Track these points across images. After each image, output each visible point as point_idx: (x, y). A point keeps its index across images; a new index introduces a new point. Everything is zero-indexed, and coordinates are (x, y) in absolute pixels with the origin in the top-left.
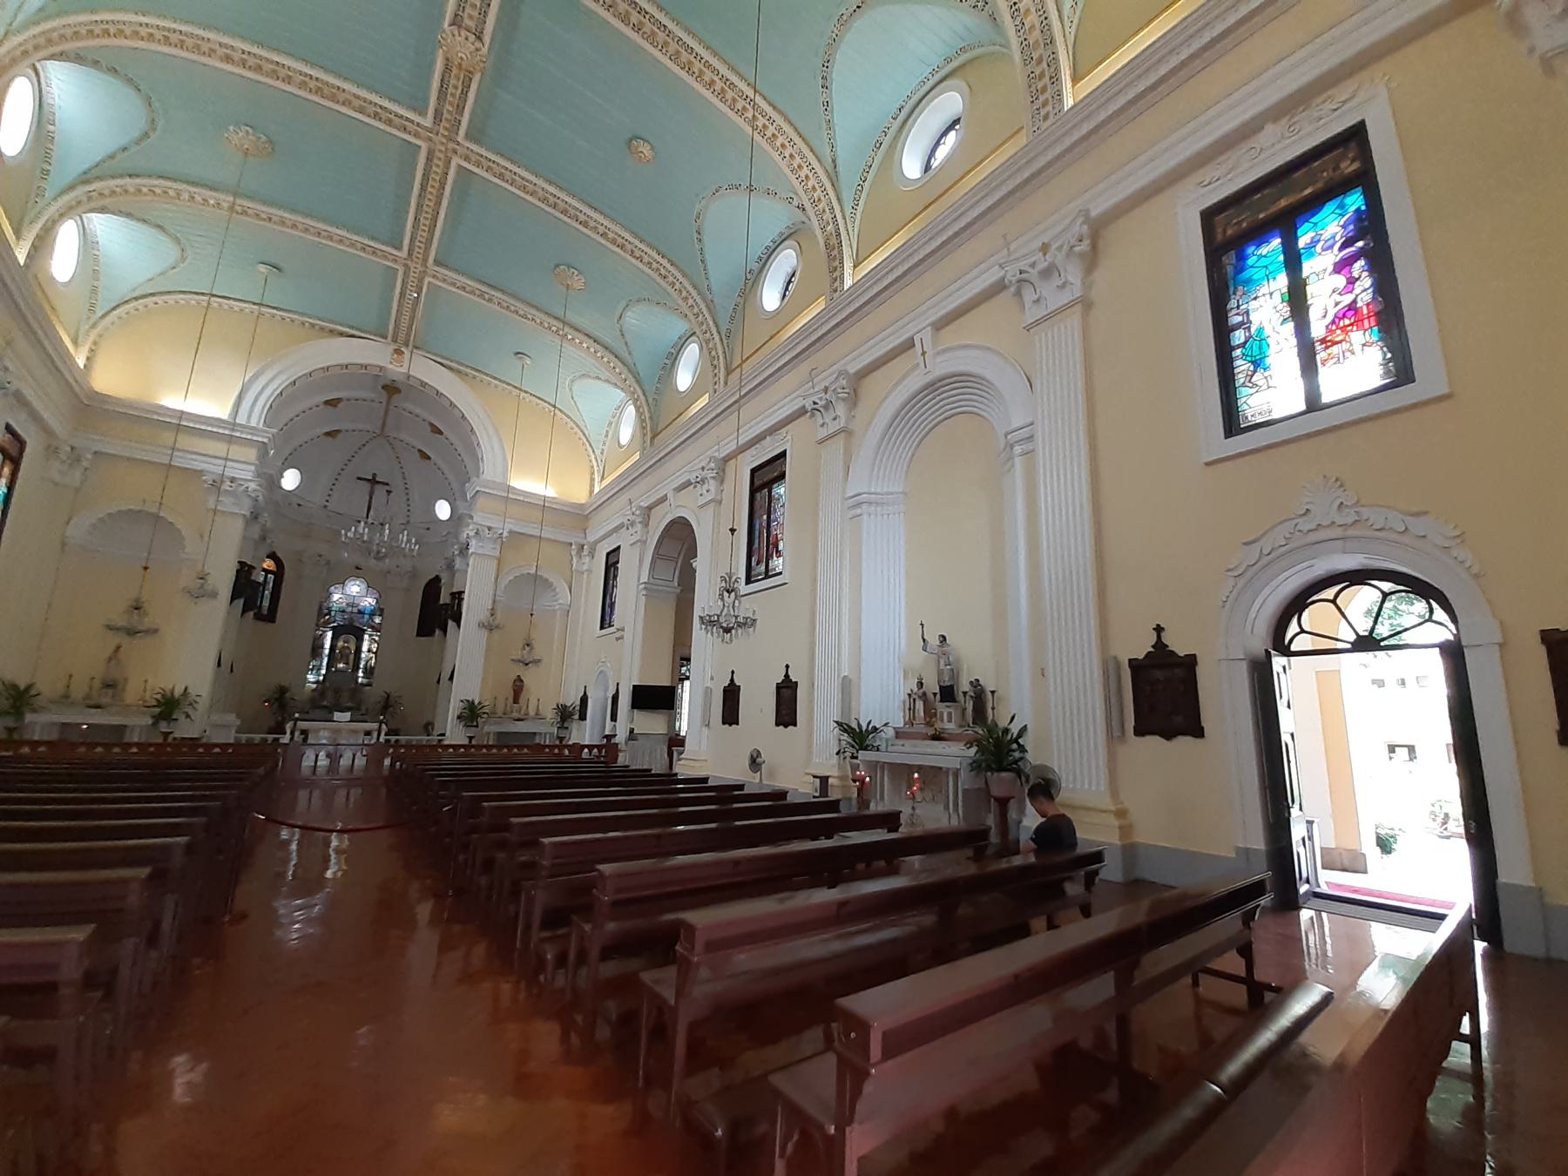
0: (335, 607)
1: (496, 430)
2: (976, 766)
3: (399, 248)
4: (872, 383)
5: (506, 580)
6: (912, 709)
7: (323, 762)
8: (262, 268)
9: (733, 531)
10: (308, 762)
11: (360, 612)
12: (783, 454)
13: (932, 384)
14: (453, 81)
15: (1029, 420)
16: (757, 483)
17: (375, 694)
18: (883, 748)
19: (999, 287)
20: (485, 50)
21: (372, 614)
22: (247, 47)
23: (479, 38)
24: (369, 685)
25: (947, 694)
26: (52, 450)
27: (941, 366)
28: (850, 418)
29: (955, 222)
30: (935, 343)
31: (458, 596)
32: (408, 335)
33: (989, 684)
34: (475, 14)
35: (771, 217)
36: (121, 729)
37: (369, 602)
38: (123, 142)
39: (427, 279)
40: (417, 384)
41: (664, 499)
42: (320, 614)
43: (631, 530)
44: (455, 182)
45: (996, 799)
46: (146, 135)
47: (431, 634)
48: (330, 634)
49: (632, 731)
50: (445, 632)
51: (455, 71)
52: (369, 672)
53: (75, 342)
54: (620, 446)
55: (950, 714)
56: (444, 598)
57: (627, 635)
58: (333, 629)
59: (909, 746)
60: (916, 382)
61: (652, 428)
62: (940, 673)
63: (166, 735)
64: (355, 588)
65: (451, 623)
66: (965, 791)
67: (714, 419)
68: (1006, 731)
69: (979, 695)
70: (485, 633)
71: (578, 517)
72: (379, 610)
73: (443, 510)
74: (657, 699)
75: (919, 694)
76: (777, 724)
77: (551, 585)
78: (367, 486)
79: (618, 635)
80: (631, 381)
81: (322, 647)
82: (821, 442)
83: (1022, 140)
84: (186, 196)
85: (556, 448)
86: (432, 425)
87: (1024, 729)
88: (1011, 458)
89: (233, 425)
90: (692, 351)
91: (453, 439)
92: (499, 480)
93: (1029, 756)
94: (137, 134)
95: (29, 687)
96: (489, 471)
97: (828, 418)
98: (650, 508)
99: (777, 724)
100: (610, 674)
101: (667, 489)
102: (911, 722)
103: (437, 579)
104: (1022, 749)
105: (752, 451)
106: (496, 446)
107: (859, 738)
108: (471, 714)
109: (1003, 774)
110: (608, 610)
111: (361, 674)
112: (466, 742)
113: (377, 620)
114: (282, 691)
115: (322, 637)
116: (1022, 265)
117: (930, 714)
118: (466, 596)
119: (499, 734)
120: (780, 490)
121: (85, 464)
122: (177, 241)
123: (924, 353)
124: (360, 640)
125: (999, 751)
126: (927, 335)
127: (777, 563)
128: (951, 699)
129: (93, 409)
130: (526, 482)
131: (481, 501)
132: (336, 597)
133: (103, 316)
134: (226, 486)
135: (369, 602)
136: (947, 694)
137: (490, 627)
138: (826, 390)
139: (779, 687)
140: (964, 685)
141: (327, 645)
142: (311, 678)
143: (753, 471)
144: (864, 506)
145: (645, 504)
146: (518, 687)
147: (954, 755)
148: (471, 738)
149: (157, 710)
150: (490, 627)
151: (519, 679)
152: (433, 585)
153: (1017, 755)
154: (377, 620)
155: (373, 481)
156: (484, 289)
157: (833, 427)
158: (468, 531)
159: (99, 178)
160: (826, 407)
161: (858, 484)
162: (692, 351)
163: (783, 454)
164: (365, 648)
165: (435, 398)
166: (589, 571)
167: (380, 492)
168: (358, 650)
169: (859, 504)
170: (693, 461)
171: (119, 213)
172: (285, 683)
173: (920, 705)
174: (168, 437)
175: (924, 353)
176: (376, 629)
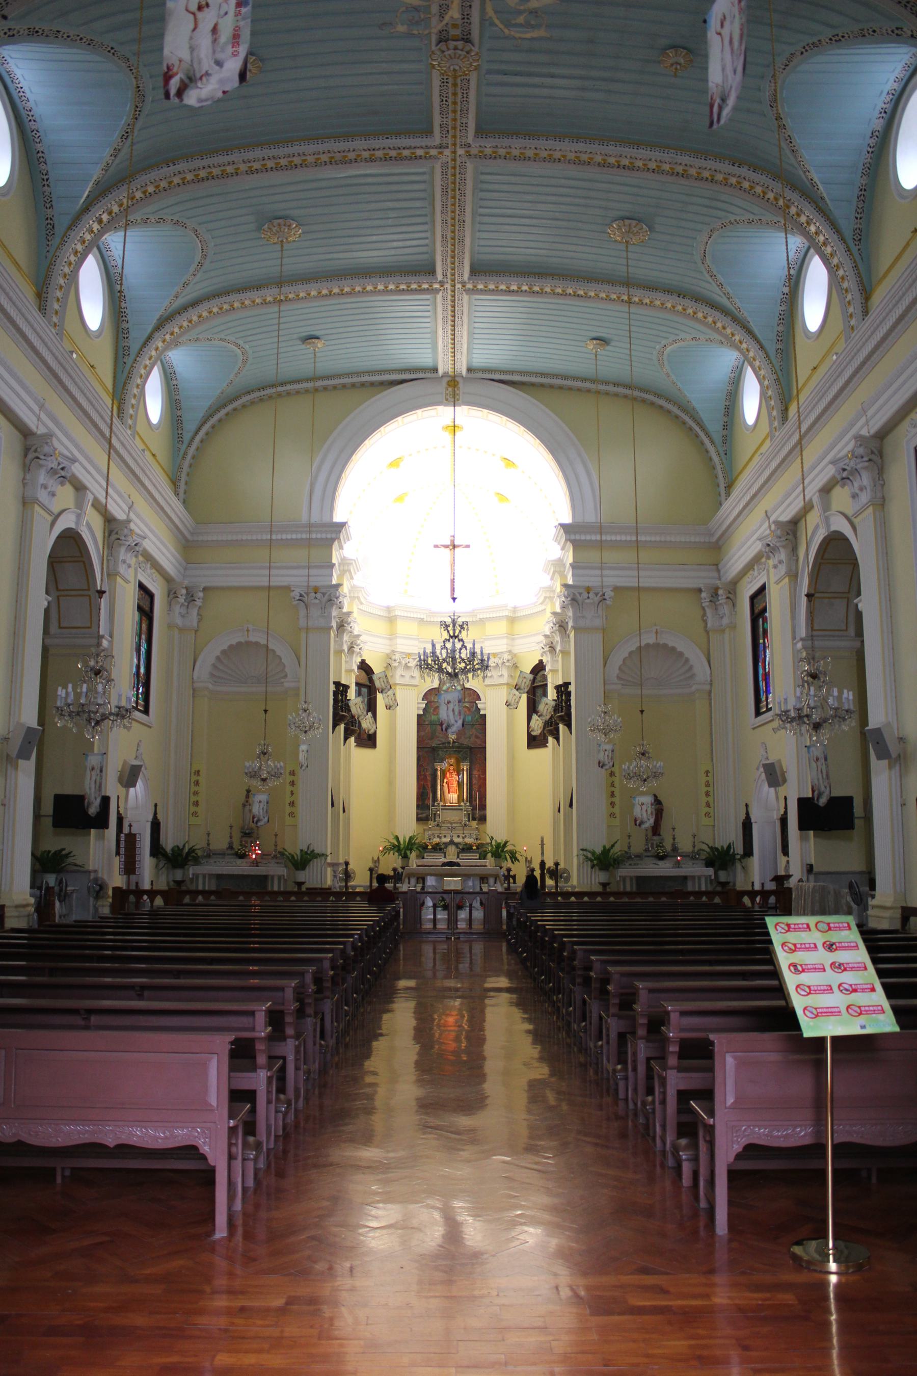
26: (172, 594)
90: (817, 277)
110: (762, 684)
112: (599, 889)
145: (786, 517)
148: (604, 885)
162: (817, 277)
166: (733, 627)
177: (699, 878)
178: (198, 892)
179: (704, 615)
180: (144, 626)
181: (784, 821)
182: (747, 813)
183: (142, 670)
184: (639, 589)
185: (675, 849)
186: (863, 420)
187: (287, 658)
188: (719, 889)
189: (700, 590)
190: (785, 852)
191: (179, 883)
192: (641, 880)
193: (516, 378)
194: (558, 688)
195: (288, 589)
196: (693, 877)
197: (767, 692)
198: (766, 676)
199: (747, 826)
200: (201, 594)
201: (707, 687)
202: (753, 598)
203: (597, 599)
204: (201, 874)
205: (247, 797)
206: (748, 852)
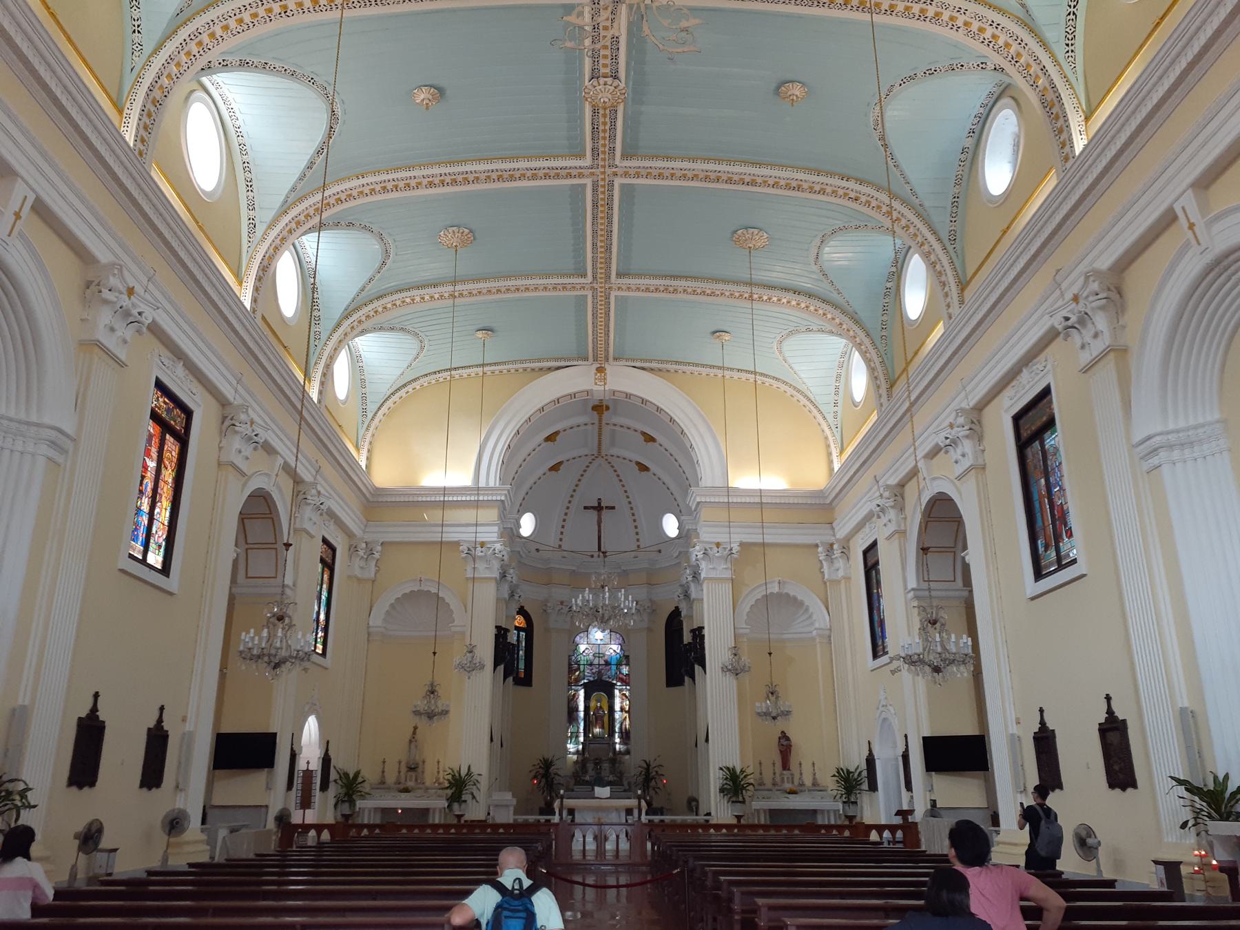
1: (708, 426)
3: (584, 275)
4: (1139, 279)
5: (745, 607)
7: (591, 846)
10: (577, 846)
11: (607, 663)
12: (1046, 392)
13: (1218, 262)
14: (601, 120)
16: (1025, 434)
17: (633, 765)
20: (622, 85)
21: (619, 664)
22: (443, 170)
23: (616, 78)
24: (628, 752)
26: (353, 549)
28: (1117, 328)
30: (1204, 207)
31: (698, 633)
32: (607, 351)
34: (608, 61)
35: (971, 90)
36: (425, 812)
37: (613, 649)
38: (369, 275)
39: (613, 294)
40: (622, 397)
42: (571, 671)
43: (884, 520)
44: (621, 201)
46: (384, 263)
47: (680, 683)
48: (582, 693)
49: (934, 803)
50: (693, 677)
51: (601, 112)
52: (625, 736)
53: (357, 448)
54: (855, 405)
56: (687, 638)
58: (585, 686)
60: (1192, 266)
61: (887, 379)
63: (459, 817)
65: (697, 668)
67: (958, 351)
70: (730, 681)
71: (817, 508)
72: (625, 659)
73: (670, 525)
74: (958, 754)
77: (801, 604)
81: (577, 710)
82: (1087, 369)
84: (418, 299)
85: (781, 429)
86: (644, 434)
91: (667, 444)
92: (719, 483)
94: (377, 265)
95: (357, 774)
96: (708, 475)
97: (1087, 334)
98: (902, 485)
100: (895, 722)
103: (676, 613)
105: (1008, 392)
106: (709, 441)
110: (878, 630)
111: (617, 740)
112: (734, 821)
113: (625, 670)
114: (547, 764)
115: (572, 700)
118: (706, 632)
120: (1050, 441)
122: (416, 335)
123: (1191, 226)
124: (611, 697)
131: (704, 514)
132: (582, 648)
133: (372, 419)
135: (613, 649)
137: (735, 670)
138: (1076, 299)
142: (571, 747)
143: (1017, 419)
144: (1163, 454)
145: (893, 481)
146: (785, 747)
148: (739, 818)
149: (449, 792)
150: (735, 670)
151: (784, 736)
154: (625, 670)
155: (599, 508)
156: (667, 282)
157: (1097, 347)
158: (697, 552)
159: (357, 309)
161: (1148, 423)
163: (1046, 392)
164: (617, 707)
165: (642, 407)
166: (847, 578)
169: (1155, 451)
170: (938, 418)
171: (374, 330)
172: (549, 756)
175: (1191, 226)
176: (625, 682)
177: (828, 811)
178: (363, 826)
179: (822, 567)
180: (326, 577)
181: (905, 757)
182: (870, 750)
183: (322, 617)
184: (763, 545)
185: (802, 785)
186: (963, 394)
187: (453, 603)
188: (847, 823)
189: (817, 546)
190: (909, 786)
191: (346, 817)
192: (773, 813)
193: (654, 365)
194: (693, 631)
195: (457, 544)
196: (822, 811)
197: (883, 637)
198: (882, 623)
199: (870, 761)
200: (379, 548)
201: (827, 632)
202: (865, 553)
203: (727, 552)
204: (368, 807)
205: (414, 733)
206: (873, 787)
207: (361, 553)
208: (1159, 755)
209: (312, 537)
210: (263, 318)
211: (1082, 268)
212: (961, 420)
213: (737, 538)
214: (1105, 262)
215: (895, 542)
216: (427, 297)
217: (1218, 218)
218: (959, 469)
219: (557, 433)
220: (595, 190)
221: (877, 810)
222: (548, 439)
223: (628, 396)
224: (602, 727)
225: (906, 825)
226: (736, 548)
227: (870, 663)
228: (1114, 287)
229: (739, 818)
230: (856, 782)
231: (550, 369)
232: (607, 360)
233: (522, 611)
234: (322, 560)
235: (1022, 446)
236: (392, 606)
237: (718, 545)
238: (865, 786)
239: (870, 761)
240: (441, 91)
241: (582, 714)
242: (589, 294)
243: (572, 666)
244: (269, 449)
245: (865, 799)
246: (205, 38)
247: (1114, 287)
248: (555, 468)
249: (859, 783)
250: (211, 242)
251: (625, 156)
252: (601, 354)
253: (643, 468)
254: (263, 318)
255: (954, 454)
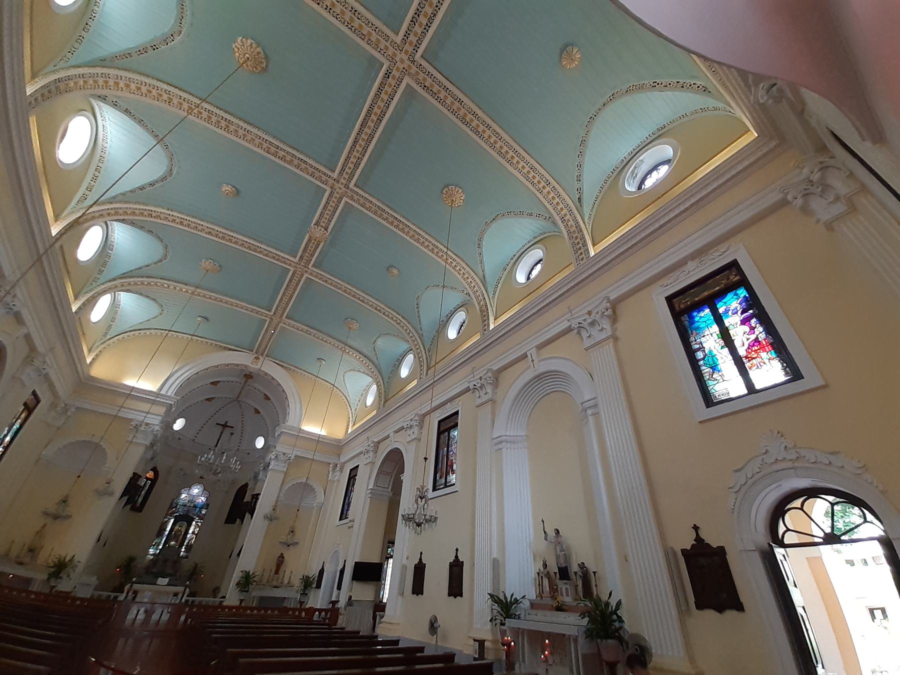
0: (181, 502)
2: (590, 634)
4: (505, 377)
5: (287, 487)
6: (541, 585)
8: (199, 319)
9: (426, 459)
11: (195, 507)
12: (457, 413)
13: (538, 376)
15: (593, 396)
16: (442, 429)
17: (187, 565)
18: (522, 616)
19: (569, 330)
21: (202, 508)
22: (220, 229)
24: (186, 557)
25: (564, 573)
27: (542, 369)
28: (494, 393)
29: (542, 302)
31: (256, 497)
33: (591, 567)
41: (388, 437)
42: (171, 507)
43: (367, 456)
45: (607, 663)
47: (233, 522)
48: (172, 520)
52: (189, 548)
55: (567, 589)
56: (247, 498)
57: (356, 525)
58: (176, 518)
59: (540, 615)
60: (529, 375)
61: (384, 397)
62: (558, 557)
64: (196, 491)
65: (247, 515)
66: (584, 656)
68: (607, 604)
69: (586, 576)
70: (267, 522)
71: (336, 447)
72: (206, 506)
73: (260, 443)
75: (544, 574)
76: (449, 595)
77: (314, 489)
78: (220, 428)
79: (350, 524)
80: (376, 372)
81: (165, 530)
83: (572, 268)
85: (331, 409)
86: (265, 395)
87: (619, 603)
88: (586, 417)
89: (157, 394)
90: (410, 358)
93: (626, 626)
96: (291, 421)
97: (482, 393)
98: (379, 442)
99: (449, 595)
101: (390, 431)
102: (540, 595)
103: (246, 485)
104: (620, 619)
107: (505, 607)
108: (246, 582)
109: (610, 641)
113: (203, 512)
115: (167, 522)
116: (580, 320)
117: (554, 590)
118: (261, 497)
119: (262, 599)
120: (455, 433)
121: (69, 414)
123: (533, 361)
124: (190, 525)
125: (604, 621)
126: (534, 351)
127: (452, 478)
128: (566, 578)
129: (86, 384)
130: (312, 428)
131: (282, 438)
132: (183, 496)
134: (142, 428)
136: (564, 573)
137: (270, 518)
138: (481, 379)
139: (452, 566)
140: (575, 568)
141: (168, 529)
142: (151, 551)
143: (440, 422)
147: (571, 624)
151: (282, 556)
152: (243, 489)
153: (617, 624)
155: (225, 426)
157: (485, 398)
160: (481, 388)
162: (410, 358)
163: (457, 413)
164: (191, 531)
166: (339, 481)
167: (228, 431)
168: (187, 532)
169: (501, 442)
173: (546, 582)
174: (120, 401)
175: (533, 361)
176: (201, 518)
180: (23, 416)
181: (342, 572)
190: (339, 588)
197: (348, 510)
199: (321, 572)
206: (319, 586)
207: (59, 409)
208: (479, 585)
209: (23, 385)
210: (61, 247)
211: (487, 367)
212: (417, 418)
213: (292, 453)
214: (495, 368)
215: (368, 468)
216: (178, 288)
217: (542, 360)
218: (409, 439)
219: (219, 382)
220: (293, 274)
221: (318, 600)
222: (212, 383)
223: (266, 374)
224: (176, 541)
225: (333, 611)
226: (293, 457)
227: (337, 522)
228: (497, 376)
229: (242, 601)
230: (310, 584)
231: (230, 349)
232: (262, 355)
233: (154, 470)
234: (25, 404)
235: (439, 433)
236: (65, 446)
237: (284, 454)
238: (314, 586)
239: (321, 572)
240: (238, 192)
241: (167, 533)
242: (268, 320)
243: (173, 505)
244: (18, 318)
245: (312, 593)
246: (111, 82)
247: (497, 376)
248: (209, 400)
249: (312, 583)
250: (48, 185)
251: (313, 266)
252: (261, 350)
253: (257, 412)
254: (61, 247)
255: (409, 432)
